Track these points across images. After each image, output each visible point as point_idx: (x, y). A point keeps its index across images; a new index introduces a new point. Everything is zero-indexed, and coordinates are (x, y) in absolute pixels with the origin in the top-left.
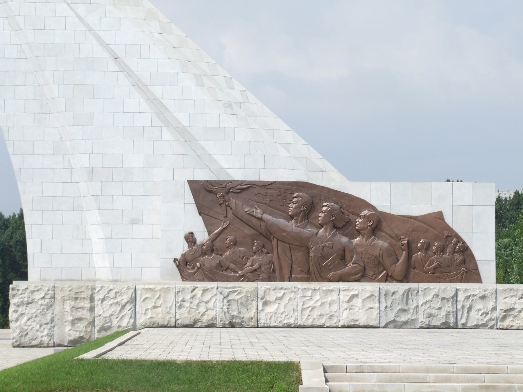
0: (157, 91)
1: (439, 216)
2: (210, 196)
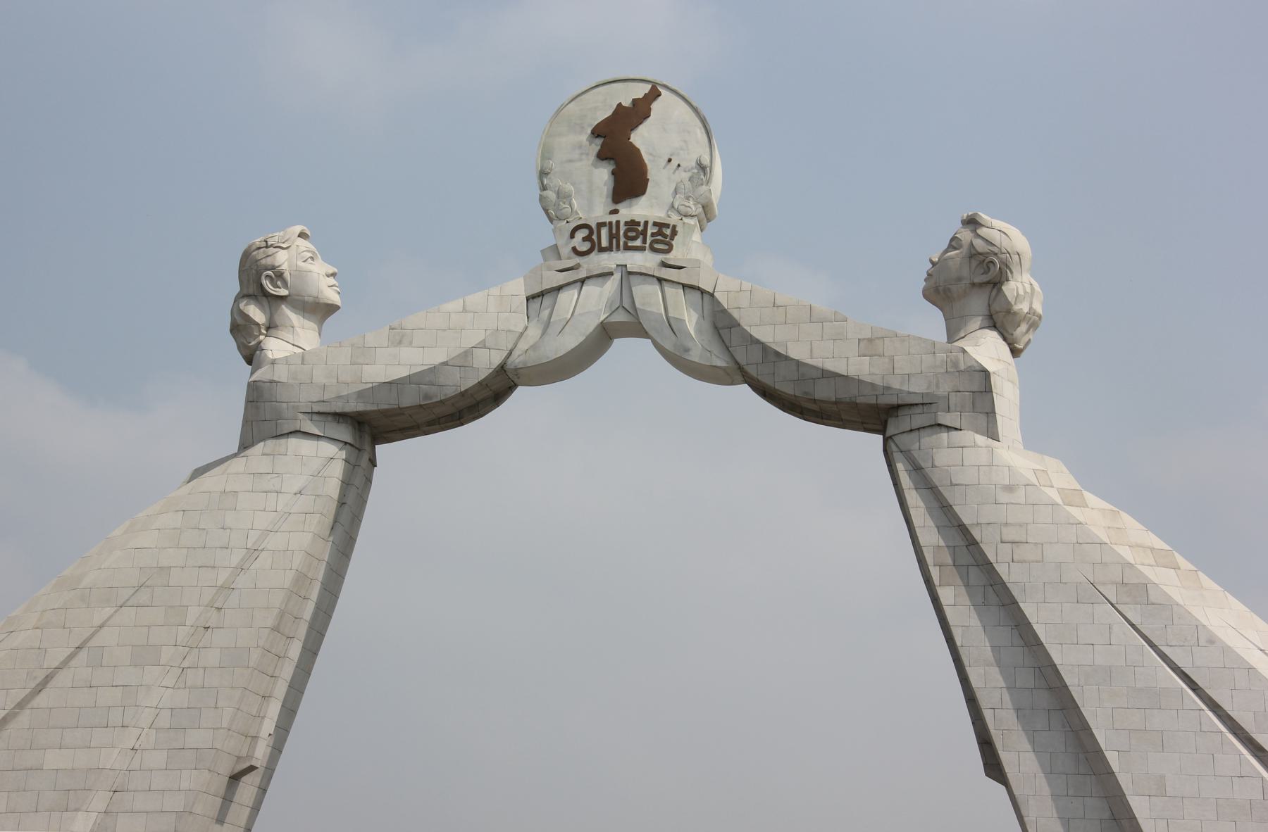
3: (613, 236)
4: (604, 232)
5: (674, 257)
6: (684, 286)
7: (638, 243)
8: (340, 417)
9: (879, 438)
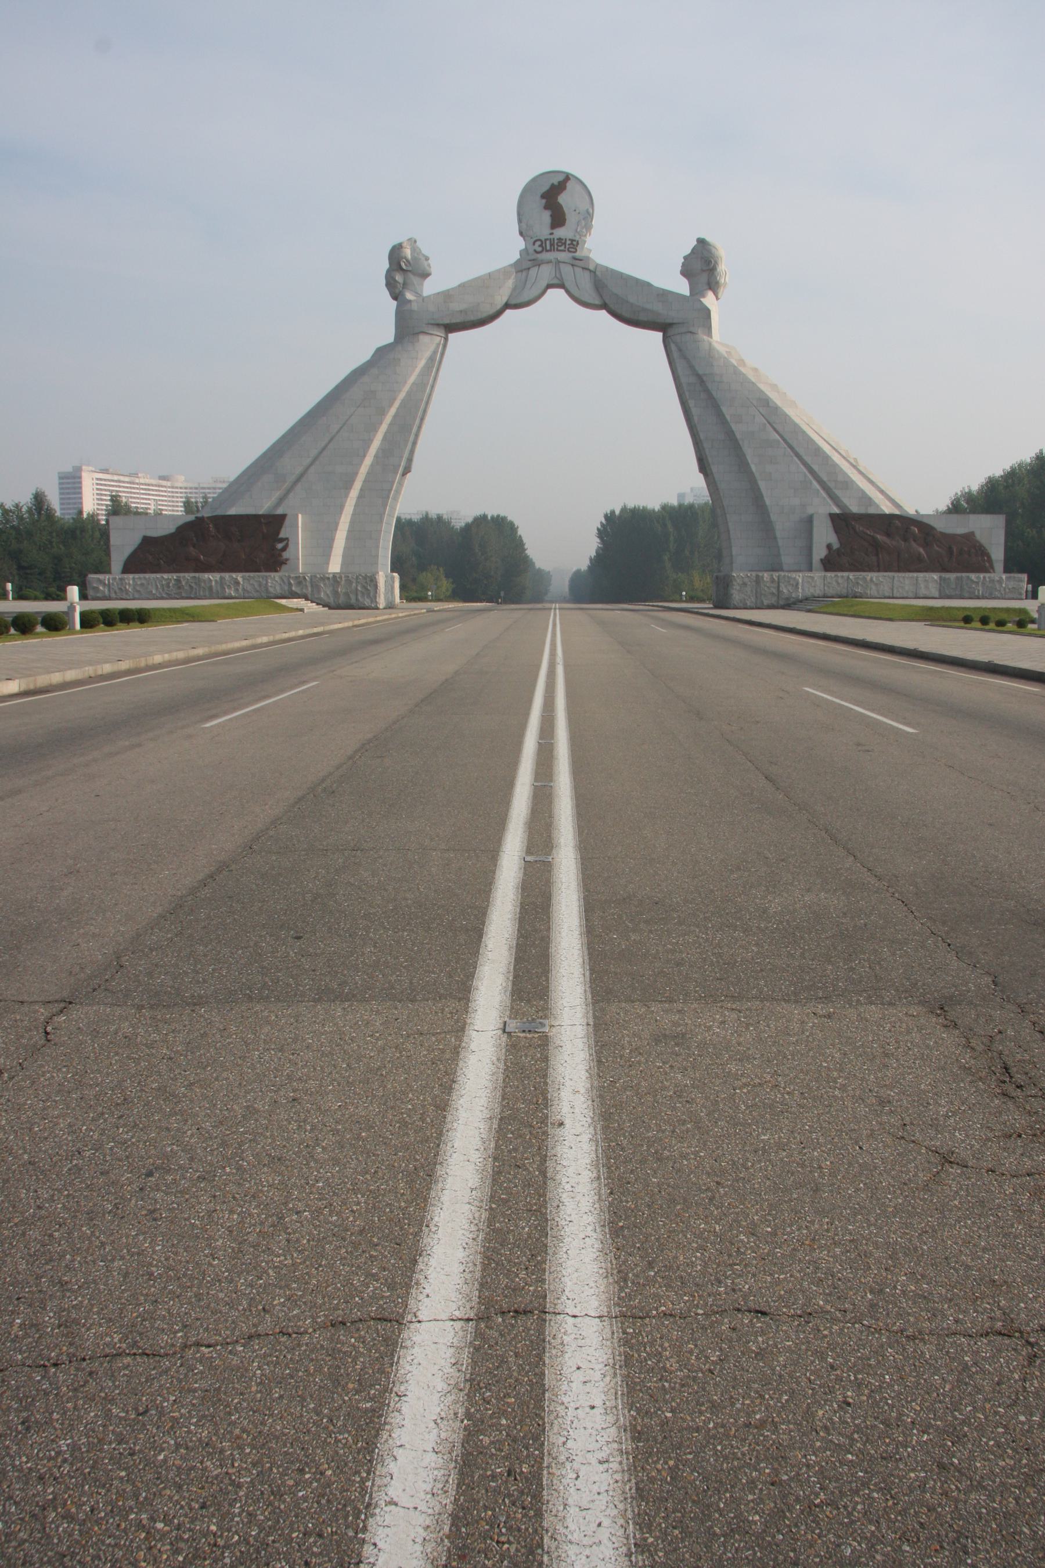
0: (808, 459)
1: (972, 534)
2: (842, 521)
3: (552, 245)
4: (548, 242)
5: (578, 254)
6: (583, 268)
7: (562, 248)
8: (438, 325)
9: (660, 335)
